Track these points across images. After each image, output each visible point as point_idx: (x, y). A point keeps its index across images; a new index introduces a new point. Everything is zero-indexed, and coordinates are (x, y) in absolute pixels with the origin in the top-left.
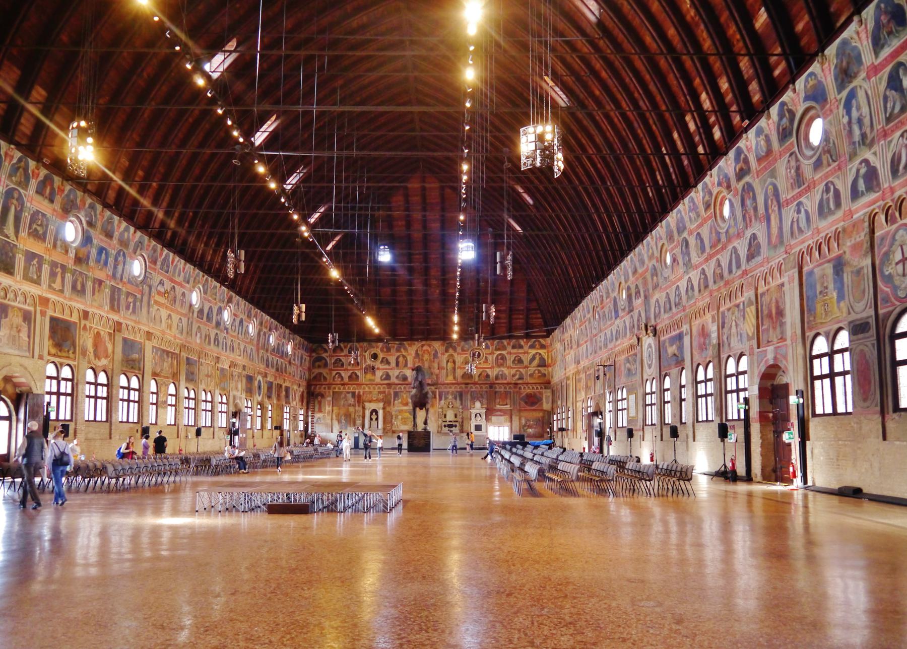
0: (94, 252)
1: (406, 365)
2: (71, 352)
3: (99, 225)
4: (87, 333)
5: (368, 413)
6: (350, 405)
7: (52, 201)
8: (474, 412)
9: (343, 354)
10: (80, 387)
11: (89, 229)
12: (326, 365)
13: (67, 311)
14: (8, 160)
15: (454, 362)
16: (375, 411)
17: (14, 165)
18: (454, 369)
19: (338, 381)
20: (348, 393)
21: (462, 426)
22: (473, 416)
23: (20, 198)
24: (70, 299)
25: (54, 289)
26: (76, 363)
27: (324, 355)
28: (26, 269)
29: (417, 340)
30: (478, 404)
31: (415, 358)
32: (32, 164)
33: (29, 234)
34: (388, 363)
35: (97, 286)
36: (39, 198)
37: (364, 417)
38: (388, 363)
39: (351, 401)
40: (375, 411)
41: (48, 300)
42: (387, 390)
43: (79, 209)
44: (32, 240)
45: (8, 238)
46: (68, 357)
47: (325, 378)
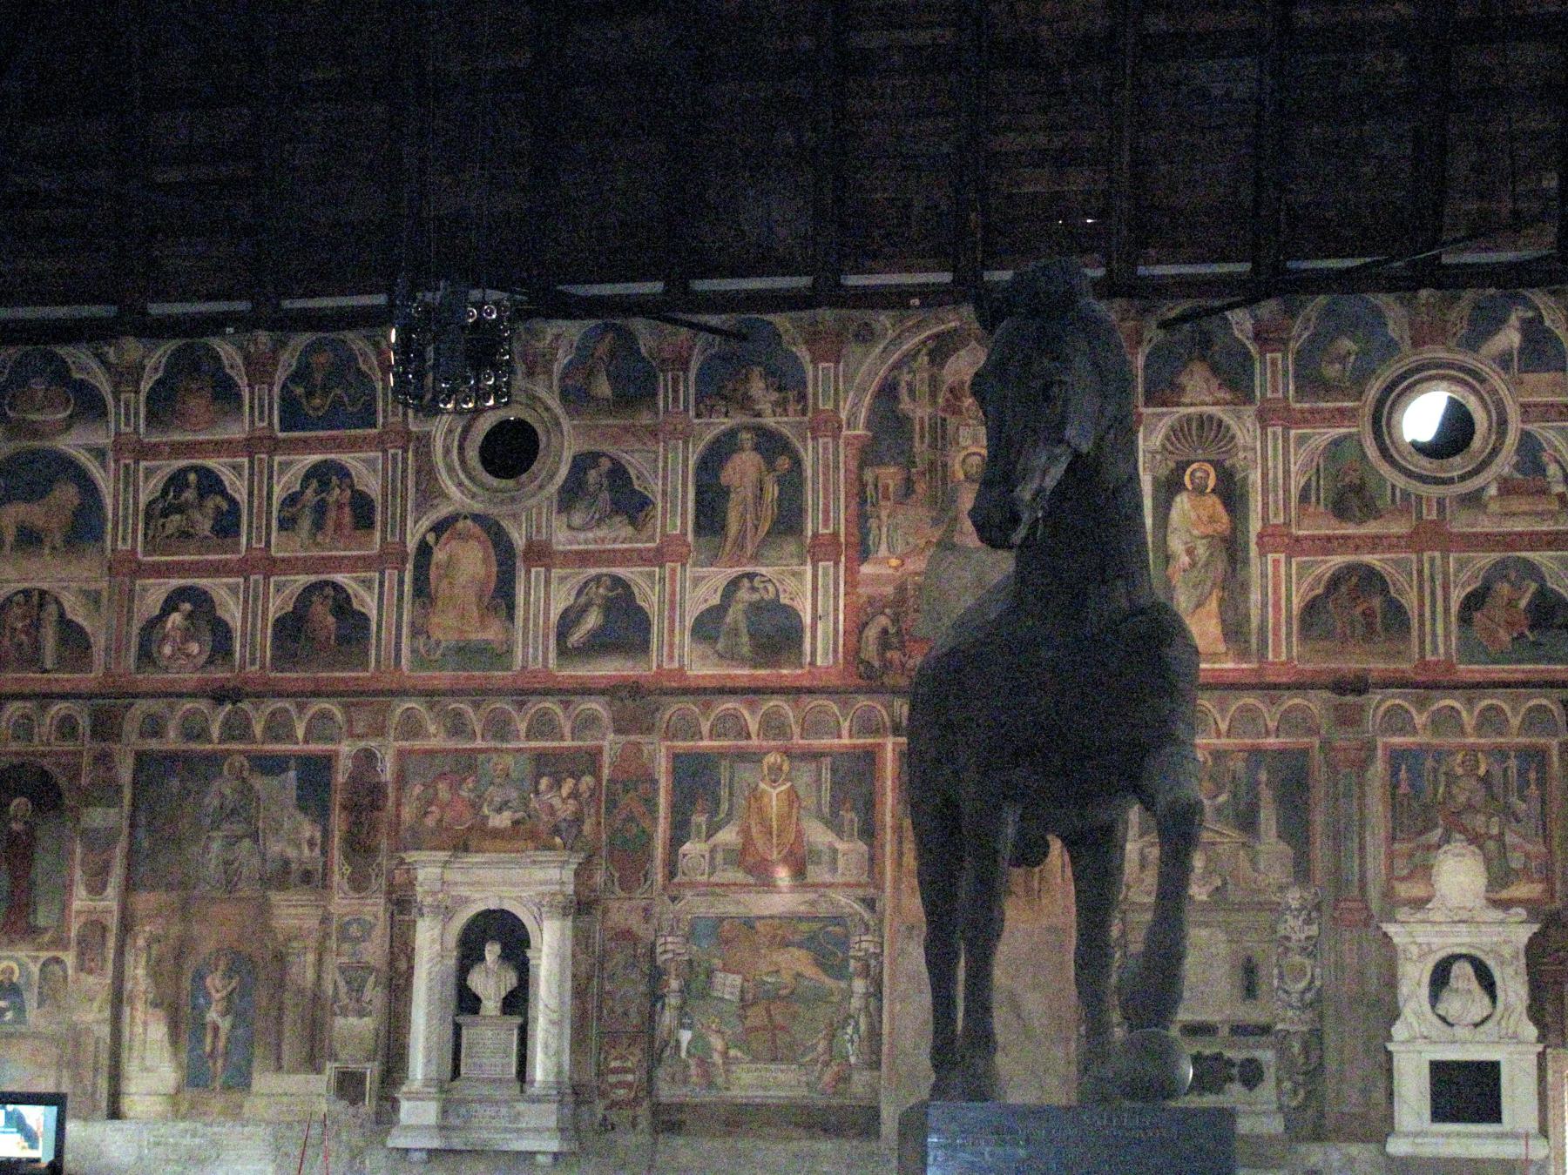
1: (788, 522)
5: (432, 944)
6: (281, 876)
8: (1418, 942)
9: (236, 431)
12: (84, 527)
15: (1231, 492)
16: (500, 933)
18: (1232, 548)
19: (184, 662)
20: (271, 765)
21: (1310, 1073)
22: (1414, 978)
27: (74, 443)
29: (896, 299)
30: (1459, 875)
31: (868, 455)
34: (630, 503)
37: (398, 986)
38: (630, 503)
39: (294, 836)
40: (500, 933)
42: (610, 743)
47: (74, 639)
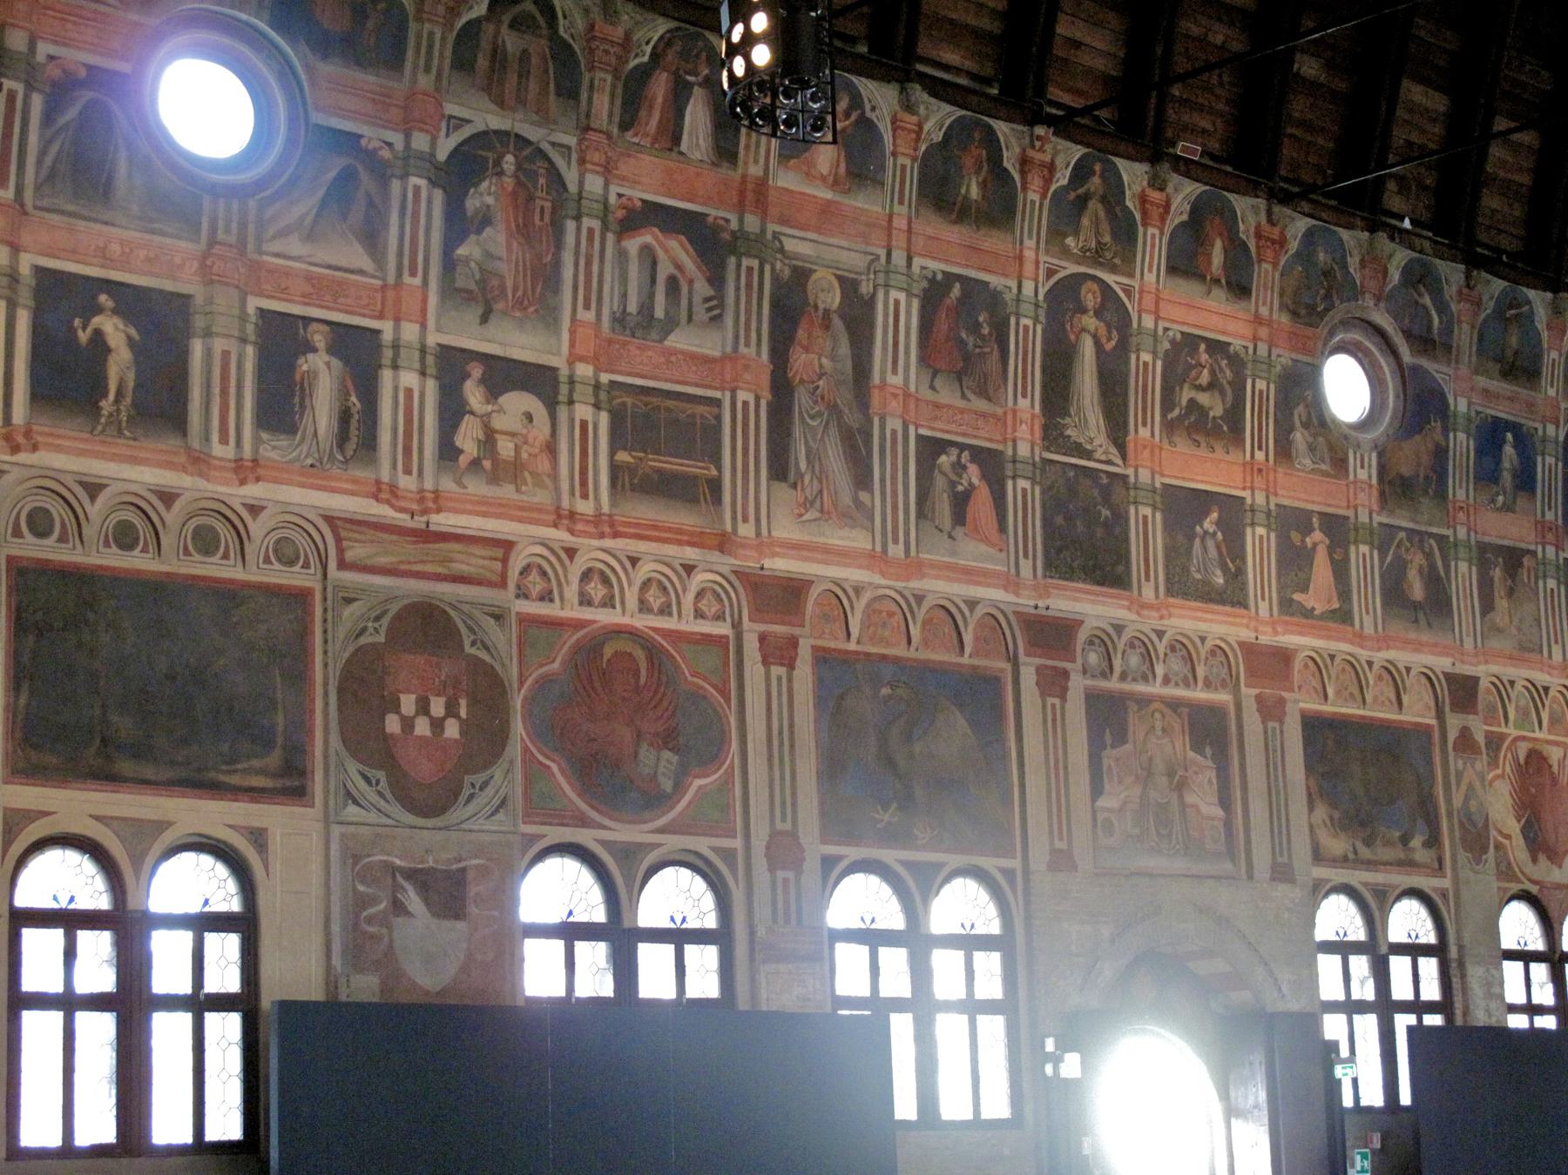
0: (1462, 443)
2: (1416, 842)
3: (1464, 336)
4: (1481, 762)
7: (1240, 289)
10: (1475, 973)
11: (1425, 363)
13: (1379, 690)
14: (1036, 182)
17: (1058, 196)
23: (1112, 308)
24: (1384, 642)
25: (1308, 613)
26: (1446, 883)
28: (1176, 556)
32: (1133, 174)
33: (1170, 427)
35: (1497, 573)
36: (1186, 289)
41: (1284, 657)
43: (1356, 293)
44: (1183, 446)
45: (1088, 455)
46: (1408, 864)
